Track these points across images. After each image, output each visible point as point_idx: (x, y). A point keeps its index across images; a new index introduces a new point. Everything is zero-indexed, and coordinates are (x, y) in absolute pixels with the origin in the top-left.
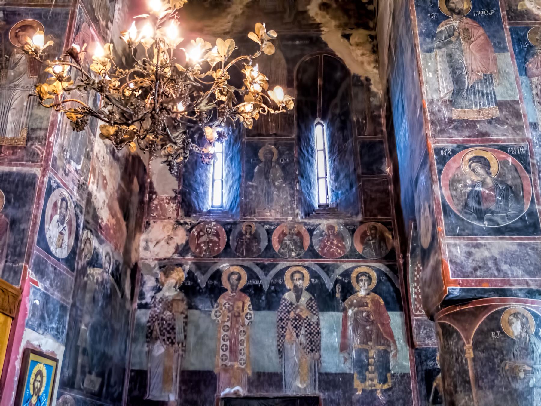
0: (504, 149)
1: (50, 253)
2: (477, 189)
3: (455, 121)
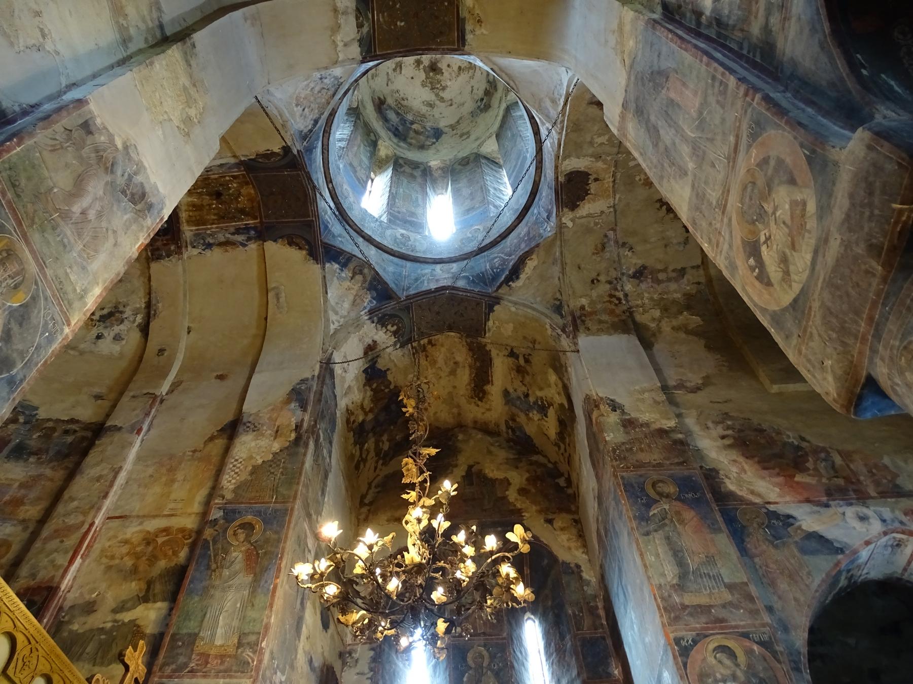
0: (746, 635)
3: (688, 606)
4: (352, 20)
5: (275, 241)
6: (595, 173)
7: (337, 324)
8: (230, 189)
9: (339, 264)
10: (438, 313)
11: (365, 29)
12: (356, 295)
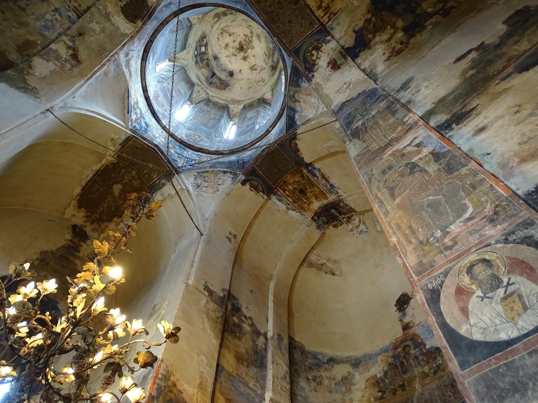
1: (509, 343)
5: (303, 158)
6: (117, 5)
8: (294, 188)
9: (294, 115)
10: (290, 22)
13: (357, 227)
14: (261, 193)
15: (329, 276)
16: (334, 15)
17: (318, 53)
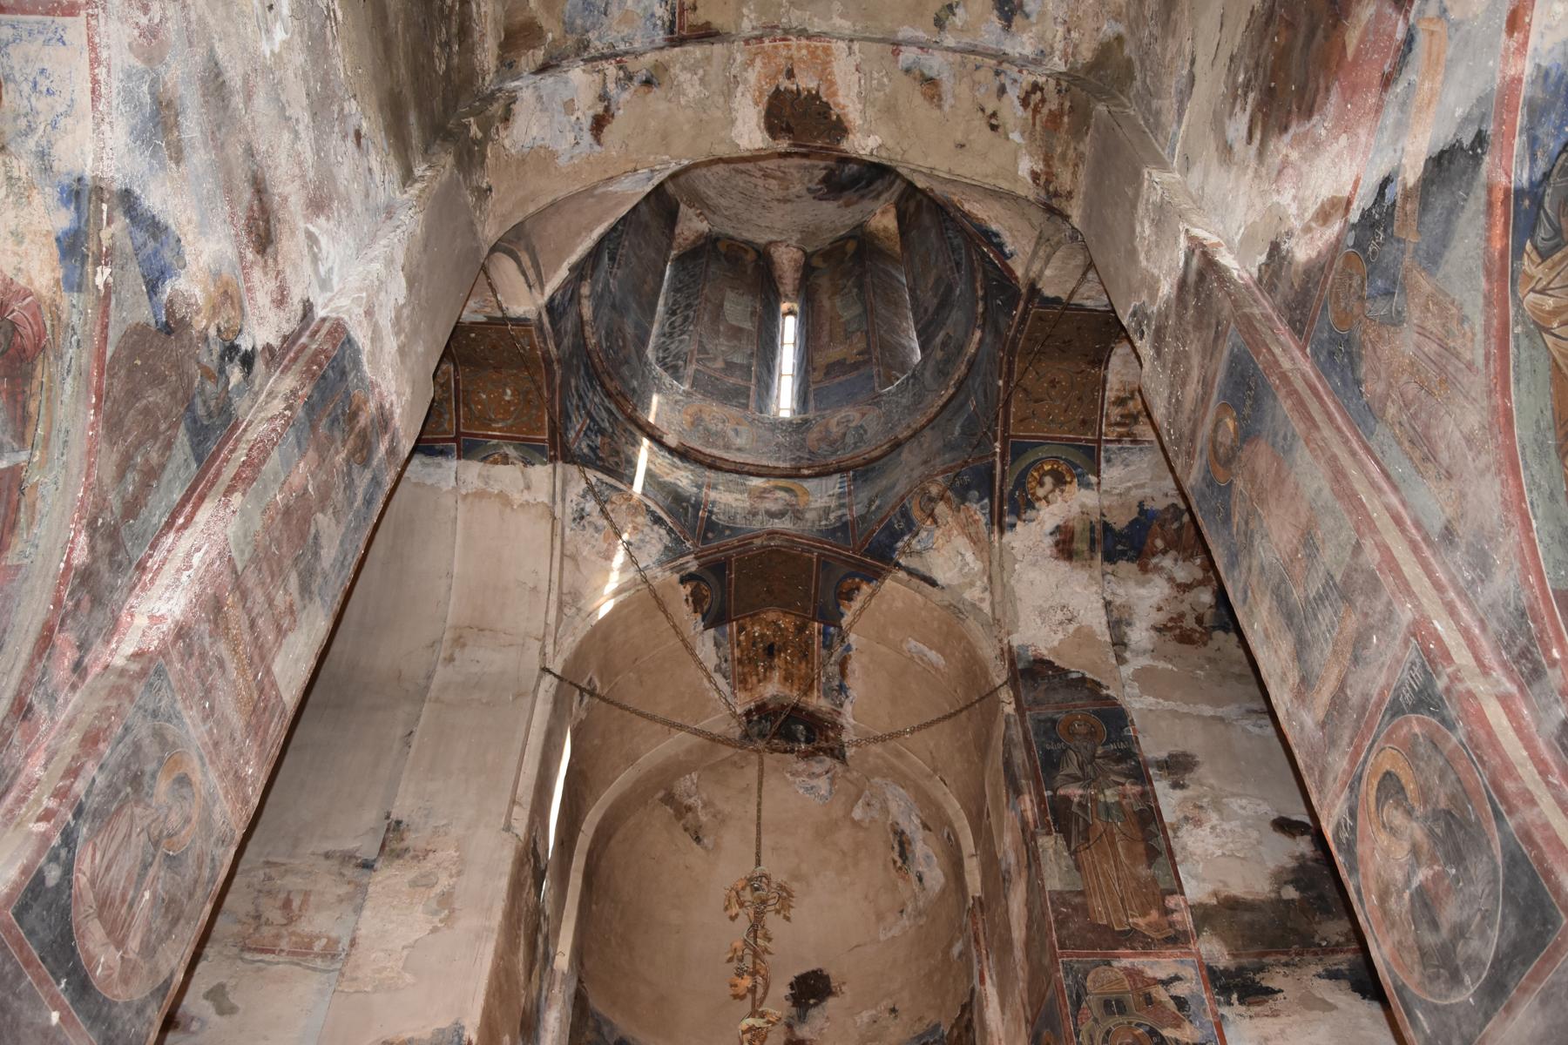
0: (1396, 710)
2: (1415, 883)
4: (500, 469)
5: (842, 615)
6: (775, 78)
7: (987, 595)
9: (903, 534)
10: (1053, 383)
11: (511, 451)
12: (963, 528)
13: (812, 775)
14: (699, 617)
15: (687, 839)
16: (1132, 442)
17: (1053, 491)
